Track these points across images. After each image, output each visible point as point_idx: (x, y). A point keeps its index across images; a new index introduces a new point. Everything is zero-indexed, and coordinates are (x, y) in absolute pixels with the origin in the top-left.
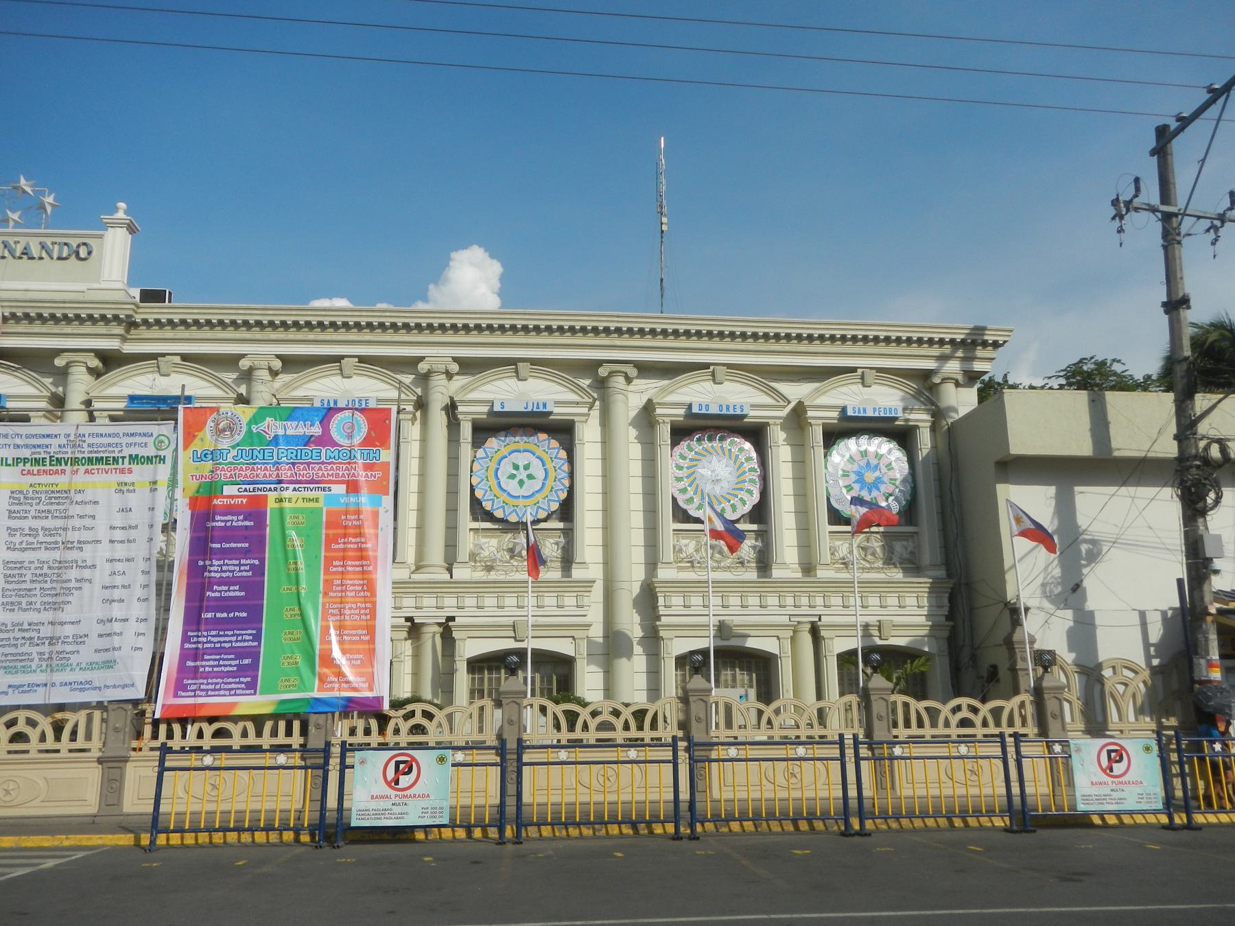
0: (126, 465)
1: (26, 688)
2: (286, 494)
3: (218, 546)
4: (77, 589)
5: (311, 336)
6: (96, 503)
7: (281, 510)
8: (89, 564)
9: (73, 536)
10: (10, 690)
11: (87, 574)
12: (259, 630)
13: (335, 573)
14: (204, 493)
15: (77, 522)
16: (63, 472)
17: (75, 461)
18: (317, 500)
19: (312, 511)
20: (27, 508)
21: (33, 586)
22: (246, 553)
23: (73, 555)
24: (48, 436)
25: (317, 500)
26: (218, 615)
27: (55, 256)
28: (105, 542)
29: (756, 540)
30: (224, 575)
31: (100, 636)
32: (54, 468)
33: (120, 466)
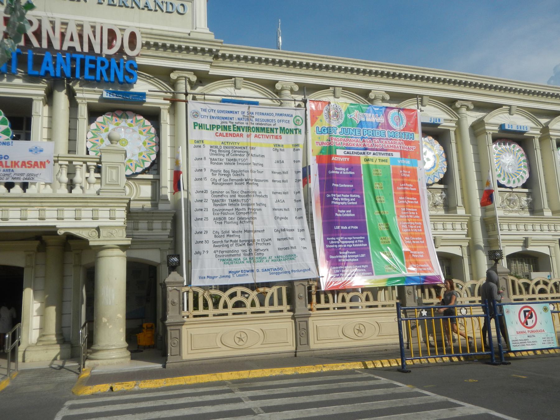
0: (279, 134)
1: (240, 273)
2: (370, 156)
3: (337, 185)
4: (258, 210)
5: (314, 73)
6: (263, 156)
7: (368, 166)
8: (263, 194)
9: (254, 176)
10: (231, 275)
11: (263, 200)
12: (366, 237)
13: (401, 204)
14: (325, 153)
15: (254, 168)
16: (242, 135)
17: (248, 129)
18: (386, 161)
19: (384, 167)
20: (222, 157)
21: (230, 208)
22: (352, 191)
23: (254, 188)
24: (231, 112)
25: (386, 161)
26: (342, 228)
27: (165, 10)
28: (270, 181)
29: (528, 197)
30: (343, 203)
31: (279, 240)
32: (236, 133)
33: (275, 134)
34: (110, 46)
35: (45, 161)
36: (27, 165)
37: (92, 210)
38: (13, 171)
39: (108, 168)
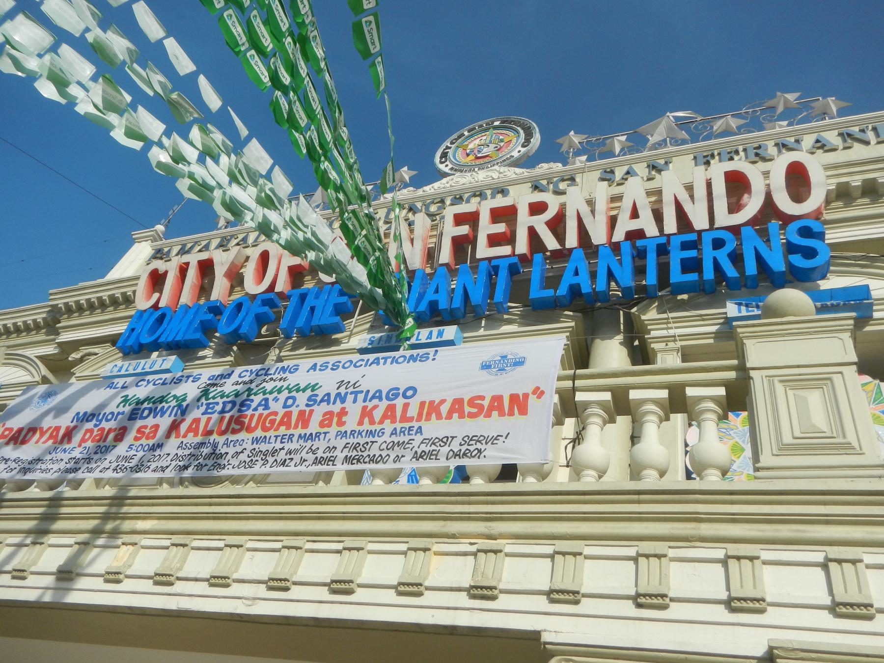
34: (734, 207)
35: (530, 392)
36: (467, 409)
37: (724, 562)
38: (420, 430)
39: (779, 388)
